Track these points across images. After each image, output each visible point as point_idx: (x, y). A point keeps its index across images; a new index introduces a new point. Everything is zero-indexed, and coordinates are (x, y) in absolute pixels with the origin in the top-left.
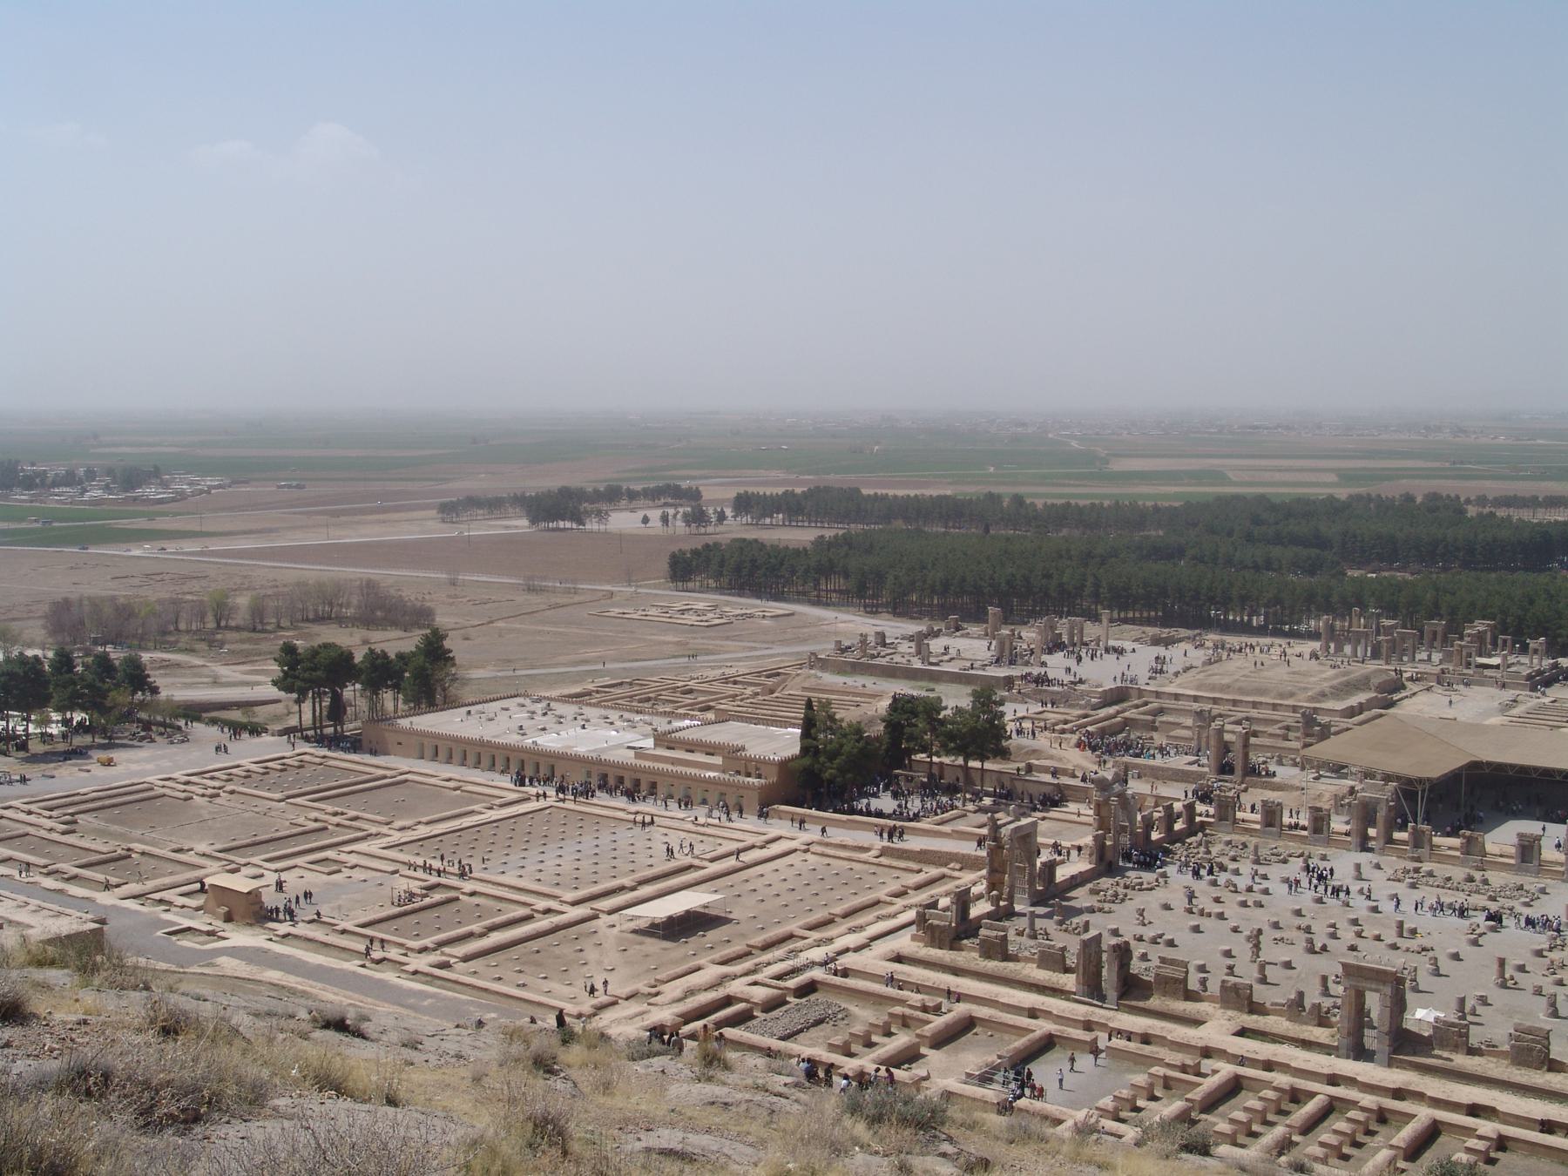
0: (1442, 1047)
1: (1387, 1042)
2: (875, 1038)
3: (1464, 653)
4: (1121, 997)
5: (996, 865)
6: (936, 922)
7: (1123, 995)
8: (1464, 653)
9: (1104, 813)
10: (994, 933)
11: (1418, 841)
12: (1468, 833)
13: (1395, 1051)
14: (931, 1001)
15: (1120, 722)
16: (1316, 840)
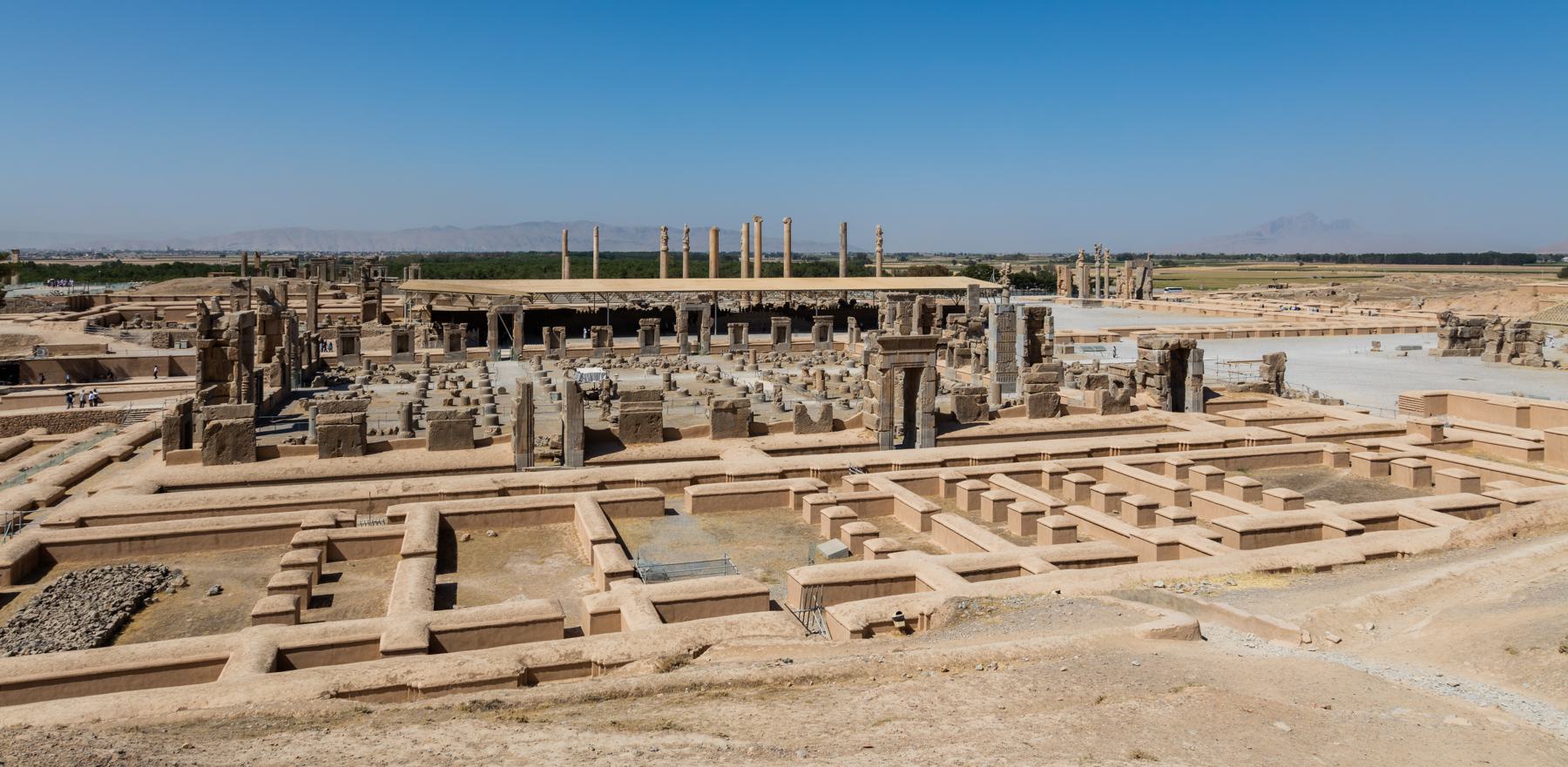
0: (965, 417)
1: (933, 424)
2: (318, 590)
3: (372, 272)
4: (587, 455)
5: (211, 371)
6: (225, 422)
7: (588, 454)
8: (372, 272)
9: (272, 329)
10: (348, 416)
11: (553, 344)
12: (598, 328)
13: (938, 434)
14: (347, 515)
15: (114, 314)
16: (454, 357)
